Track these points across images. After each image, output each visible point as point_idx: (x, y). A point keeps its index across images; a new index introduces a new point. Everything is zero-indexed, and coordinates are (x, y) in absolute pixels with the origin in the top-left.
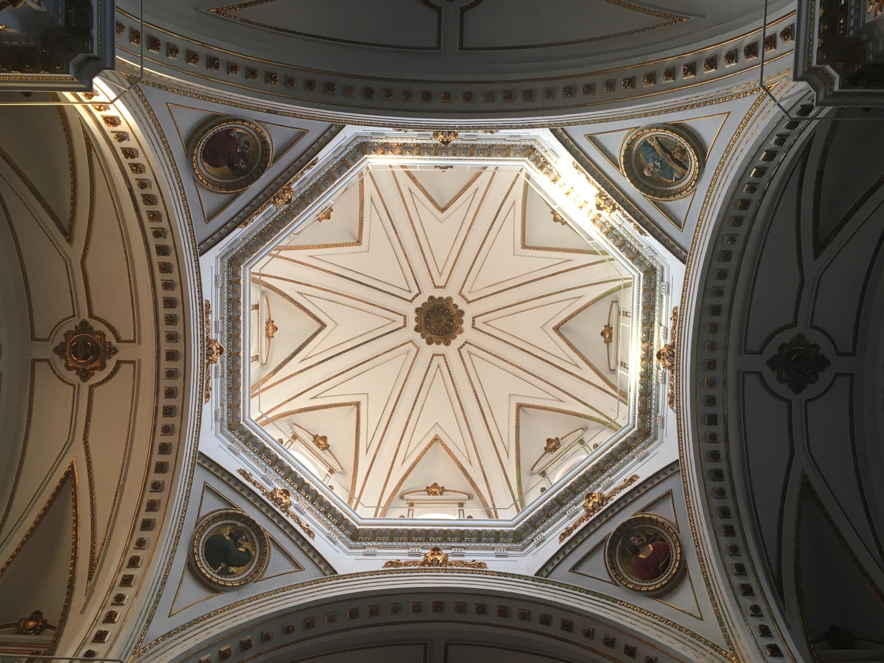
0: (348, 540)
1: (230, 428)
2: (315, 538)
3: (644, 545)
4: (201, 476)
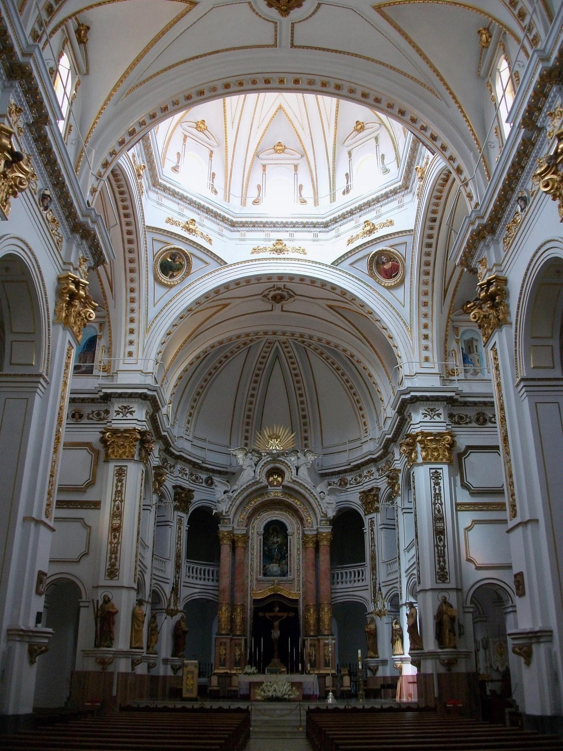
0: (229, 227)
1: (154, 186)
2: (212, 243)
3: (388, 262)
4: (149, 236)
